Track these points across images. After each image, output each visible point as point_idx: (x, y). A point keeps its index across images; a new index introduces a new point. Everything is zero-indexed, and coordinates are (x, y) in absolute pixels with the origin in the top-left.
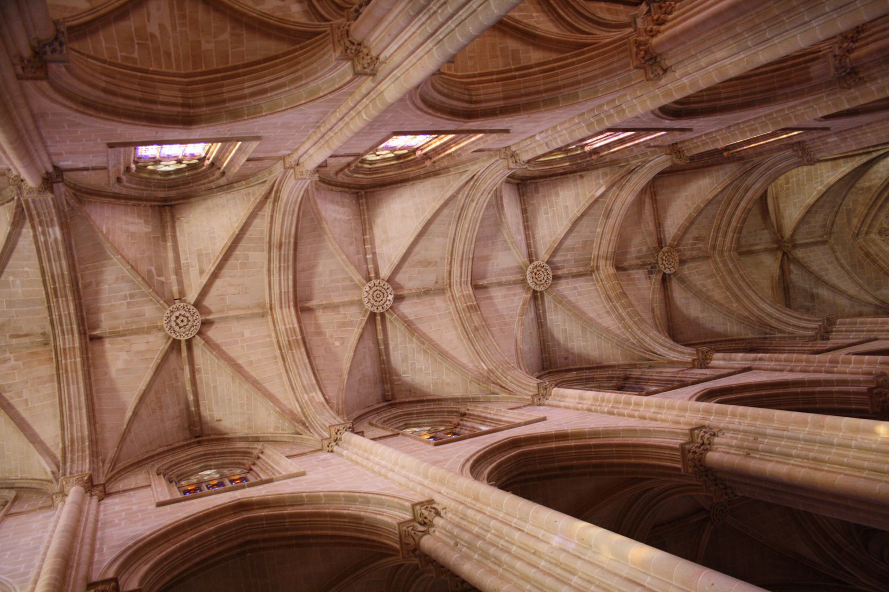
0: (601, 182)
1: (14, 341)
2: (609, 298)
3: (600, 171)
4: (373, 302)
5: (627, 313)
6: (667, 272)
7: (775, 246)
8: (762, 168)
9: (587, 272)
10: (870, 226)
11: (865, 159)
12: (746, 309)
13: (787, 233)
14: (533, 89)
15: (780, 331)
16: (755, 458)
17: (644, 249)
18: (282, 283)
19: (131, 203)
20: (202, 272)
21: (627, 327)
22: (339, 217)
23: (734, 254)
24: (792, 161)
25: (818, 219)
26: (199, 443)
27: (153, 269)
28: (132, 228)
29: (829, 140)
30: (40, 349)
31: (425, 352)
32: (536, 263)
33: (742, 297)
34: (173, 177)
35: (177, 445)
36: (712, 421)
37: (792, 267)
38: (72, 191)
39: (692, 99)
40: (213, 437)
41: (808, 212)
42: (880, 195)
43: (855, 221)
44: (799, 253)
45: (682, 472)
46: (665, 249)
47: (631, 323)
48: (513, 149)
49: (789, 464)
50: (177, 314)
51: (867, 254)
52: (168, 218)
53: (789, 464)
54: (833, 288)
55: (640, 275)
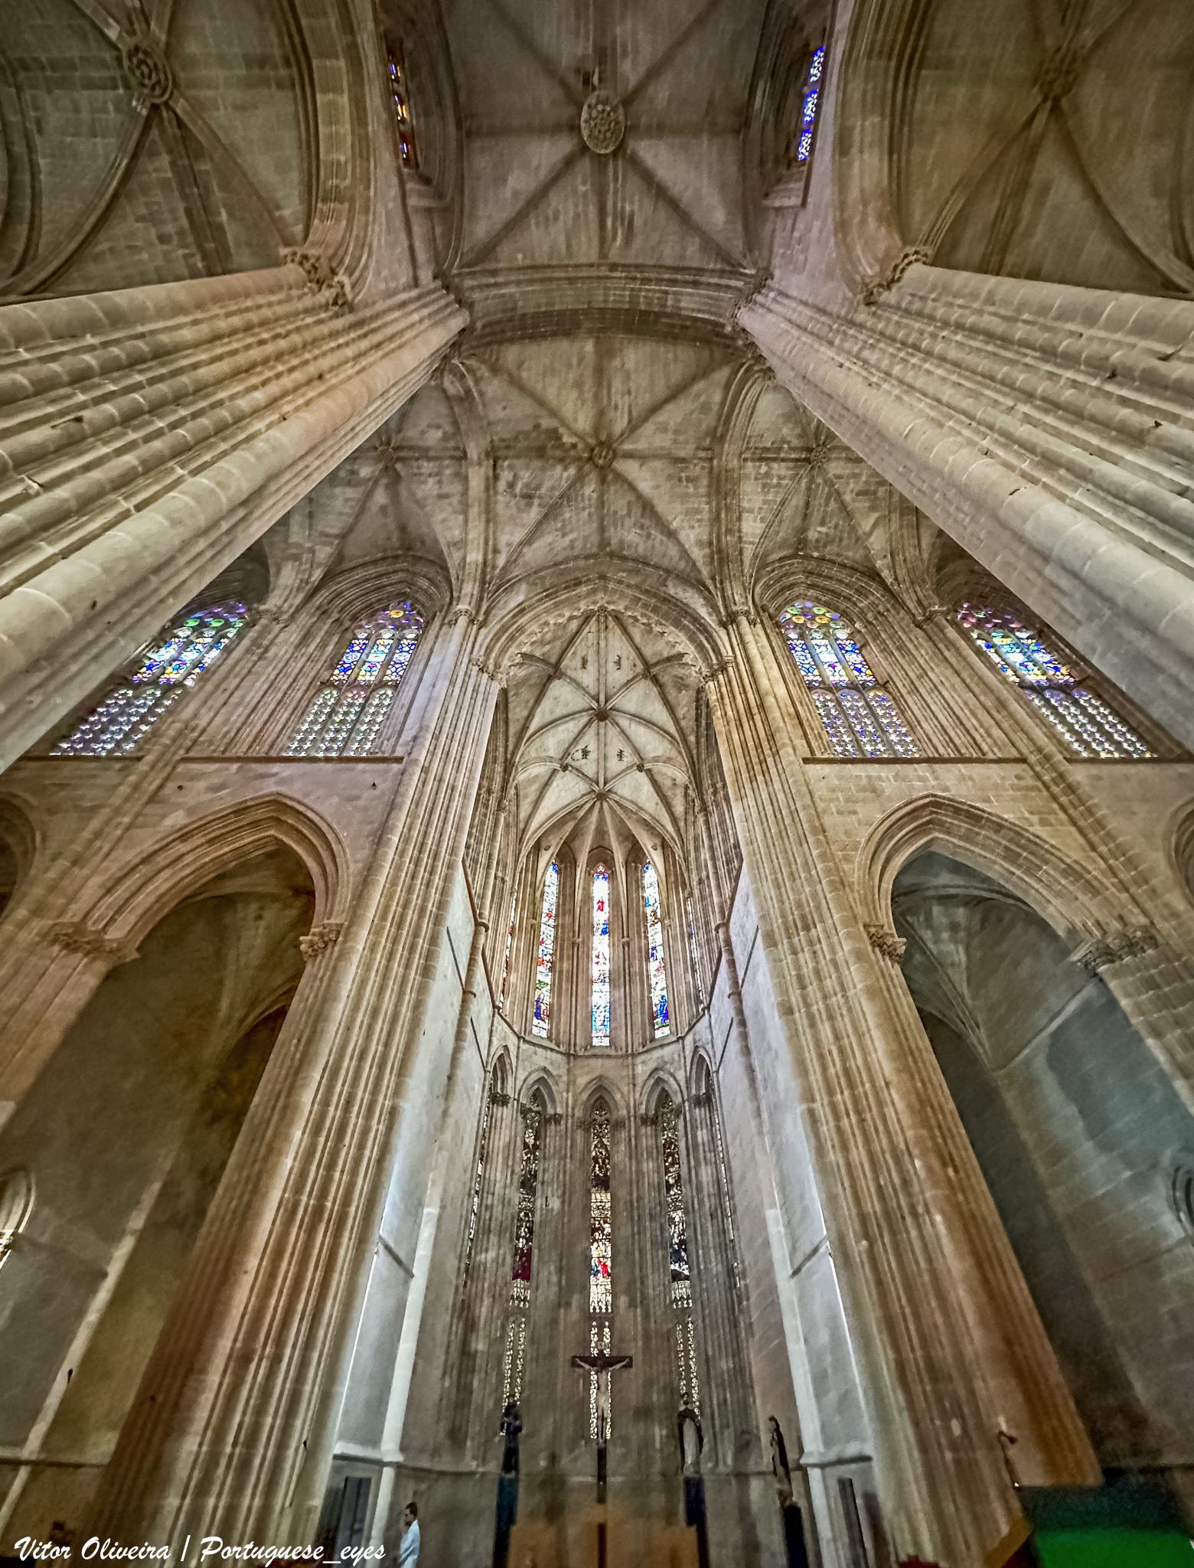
11: (705, 572)
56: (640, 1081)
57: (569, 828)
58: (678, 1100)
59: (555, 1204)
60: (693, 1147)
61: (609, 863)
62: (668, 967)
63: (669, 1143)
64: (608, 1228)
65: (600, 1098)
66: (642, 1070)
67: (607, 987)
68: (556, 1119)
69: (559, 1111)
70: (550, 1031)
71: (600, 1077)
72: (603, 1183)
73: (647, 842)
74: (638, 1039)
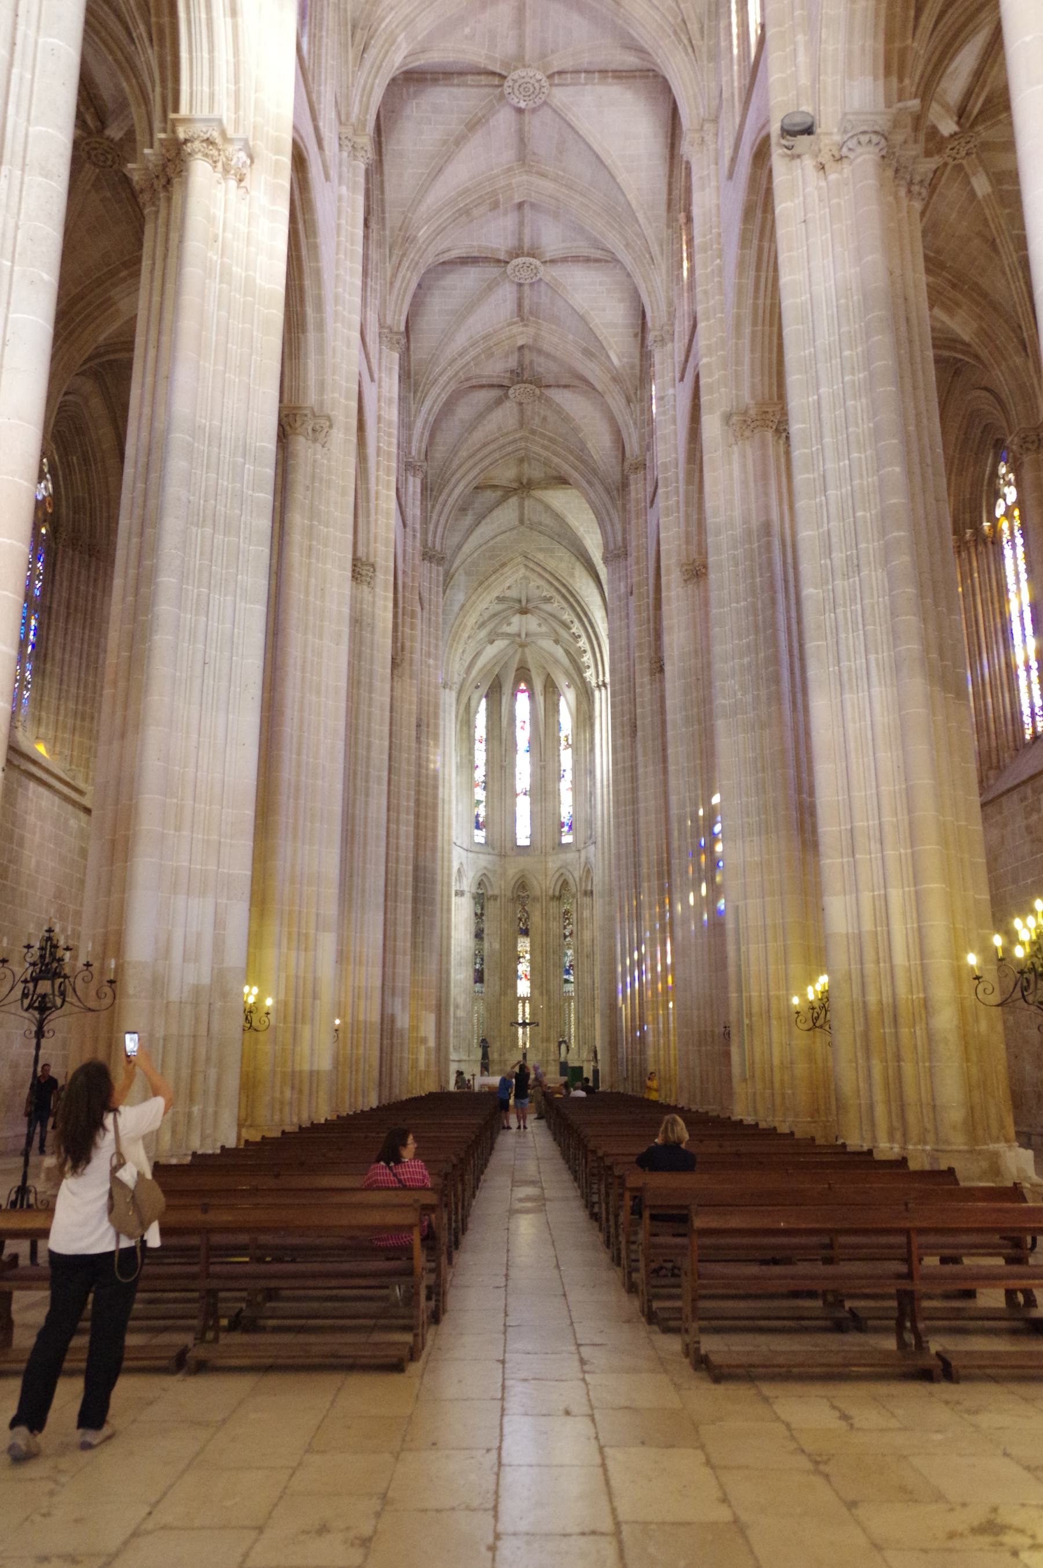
0: (625, 360)
2: (486, 337)
3: (637, 361)
4: (520, 81)
5: (468, 363)
6: (511, 391)
7: (525, 481)
8: (609, 506)
9: (521, 313)
10: (533, 570)
12: (460, 466)
13: (537, 493)
15: (433, 507)
21: (454, 360)
23: (522, 453)
24: (611, 539)
25: (547, 520)
29: (622, 585)
31: (445, 142)
32: (542, 268)
33: (471, 462)
36: (380, 576)
37: (499, 493)
39: (769, 217)
41: (557, 515)
42: (564, 585)
43: (540, 556)
44: (514, 501)
45: (172, 116)
46: (537, 391)
47: (457, 365)
48: (670, 345)
51: (503, 565)
54: (470, 531)
55: (512, 363)
56: (550, 873)
57: (497, 670)
58: (574, 890)
59: (496, 946)
60: (580, 920)
61: (529, 682)
62: (575, 789)
63: (567, 912)
64: (528, 956)
65: (522, 884)
66: (553, 864)
67: (527, 799)
68: (495, 898)
69: (496, 892)
70: (486, 838)
71: (523, 871)
72: (525, 933)
73: (562, 682)
74: (550, 844)
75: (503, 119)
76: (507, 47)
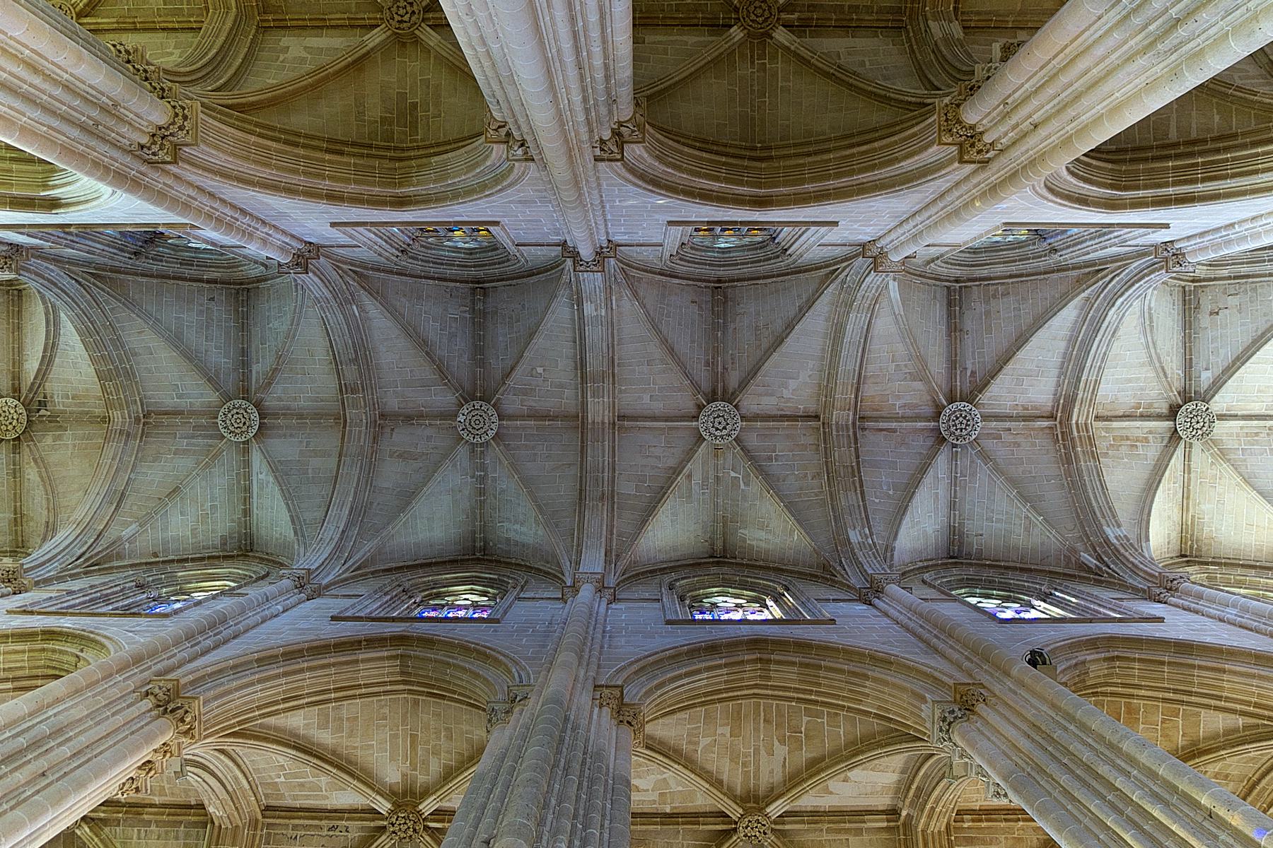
1: (894, 425)
14: (320, 673)
16: (108, 97)
17: (49, 440)
18: (598, 454)
19: (761, 563)
20: (689, 476)
22: (517, 527)
26: (719, 281)
27: (742, 486)
28: (762, 535)
30: (868, 414)
34: (715, 590)
35: (746, 283)
38: (839, 578)
40: (703, 285)
49: (71, 75)
50: (725, 432)
52: (719, 545)
53: (71, 75)
75: (443, 398)
76: (512, 403)
